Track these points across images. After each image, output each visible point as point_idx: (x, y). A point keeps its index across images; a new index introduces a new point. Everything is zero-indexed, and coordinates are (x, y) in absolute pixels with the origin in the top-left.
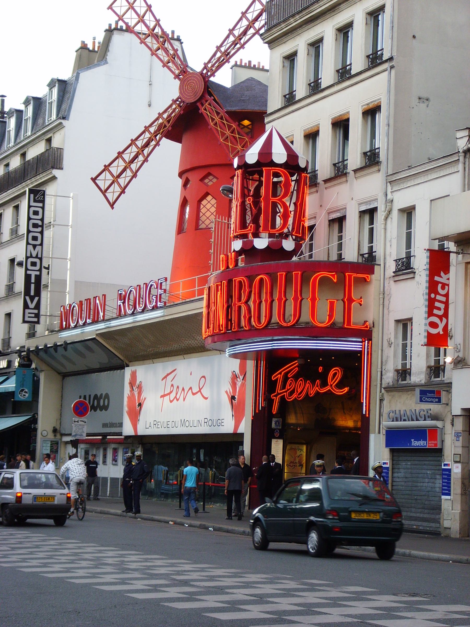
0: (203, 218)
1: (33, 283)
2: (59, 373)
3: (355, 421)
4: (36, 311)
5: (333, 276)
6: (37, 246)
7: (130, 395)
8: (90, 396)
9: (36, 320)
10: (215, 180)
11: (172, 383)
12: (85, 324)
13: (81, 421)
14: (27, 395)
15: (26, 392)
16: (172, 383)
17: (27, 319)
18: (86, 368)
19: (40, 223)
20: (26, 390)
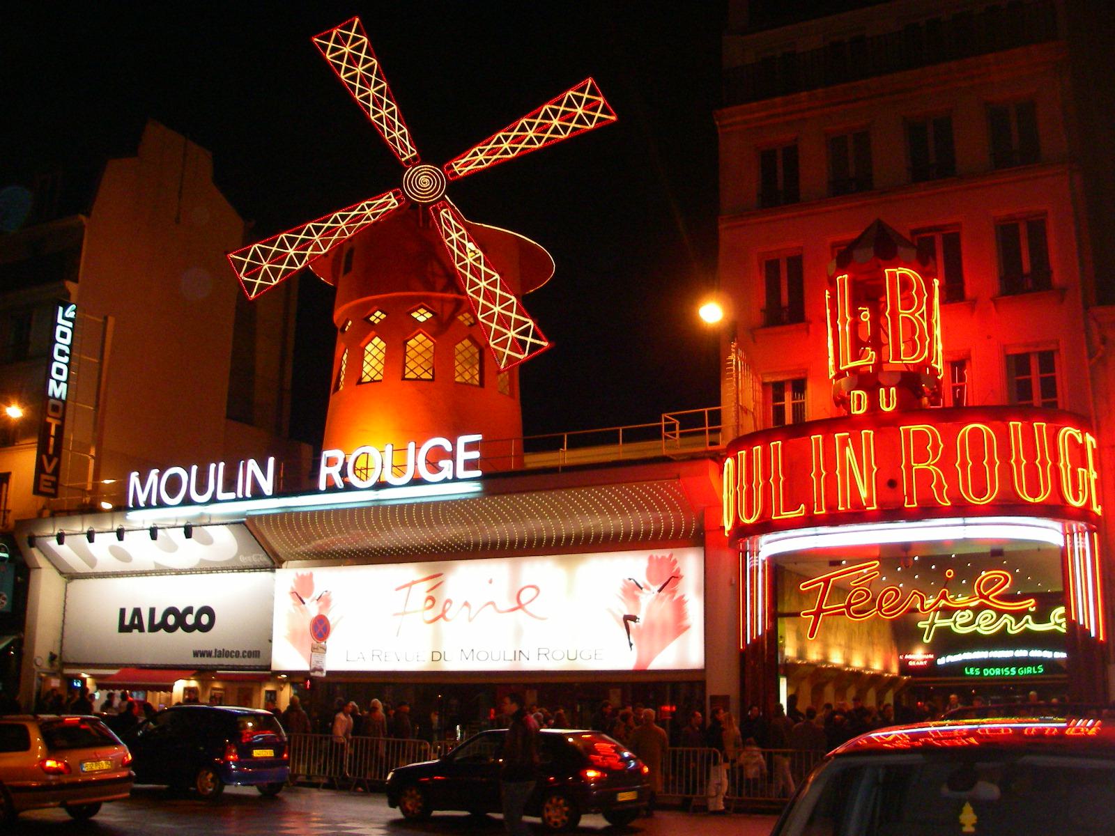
0: (411, 365)
1: (53, 437)
2: (61, 573)
3: (817, 653)
4: (53, 479)
5: (1078, 433)
6: (62, 384)
7: (294, 611)
8: (152, 611)
9: (52, 491)
10: (429, 315)
11: (431, 594)
12: (214, 500)
13: (321, 648)
14: (5, 603)
15: (4, 599)
16: (431, 594)
17: (42, 489)
18: (152, 567)
19: (67, 350)
20: (5, 596)
